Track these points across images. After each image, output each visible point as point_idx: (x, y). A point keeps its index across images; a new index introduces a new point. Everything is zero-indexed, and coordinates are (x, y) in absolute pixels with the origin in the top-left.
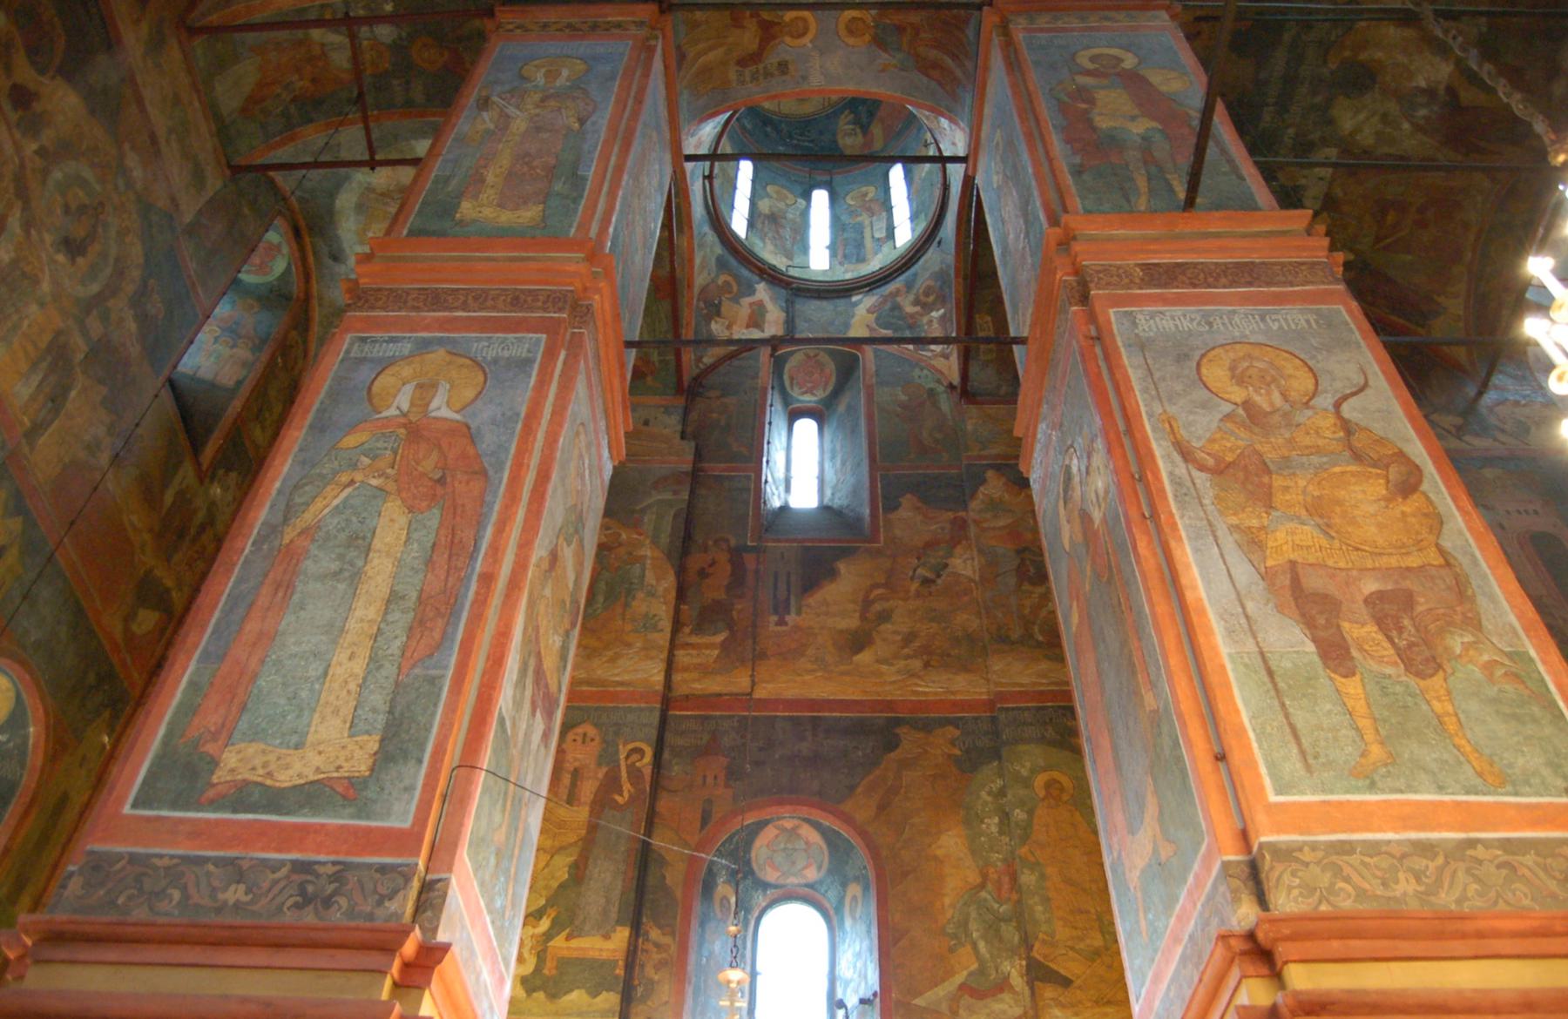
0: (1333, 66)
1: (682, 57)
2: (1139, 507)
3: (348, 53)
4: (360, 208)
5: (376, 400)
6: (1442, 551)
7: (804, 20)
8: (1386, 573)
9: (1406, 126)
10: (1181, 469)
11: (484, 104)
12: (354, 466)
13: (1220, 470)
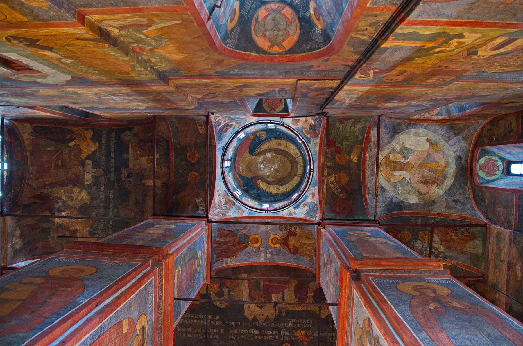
0: (94, 213)
3: (433, 239)
4: (445, 177)
7: (272, 243)
9: (64, 198)
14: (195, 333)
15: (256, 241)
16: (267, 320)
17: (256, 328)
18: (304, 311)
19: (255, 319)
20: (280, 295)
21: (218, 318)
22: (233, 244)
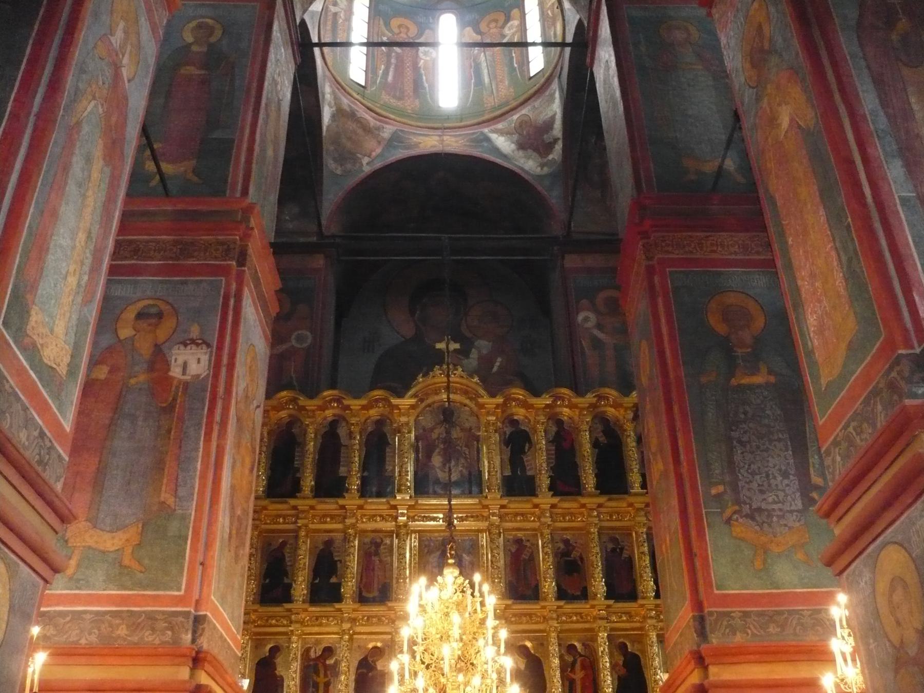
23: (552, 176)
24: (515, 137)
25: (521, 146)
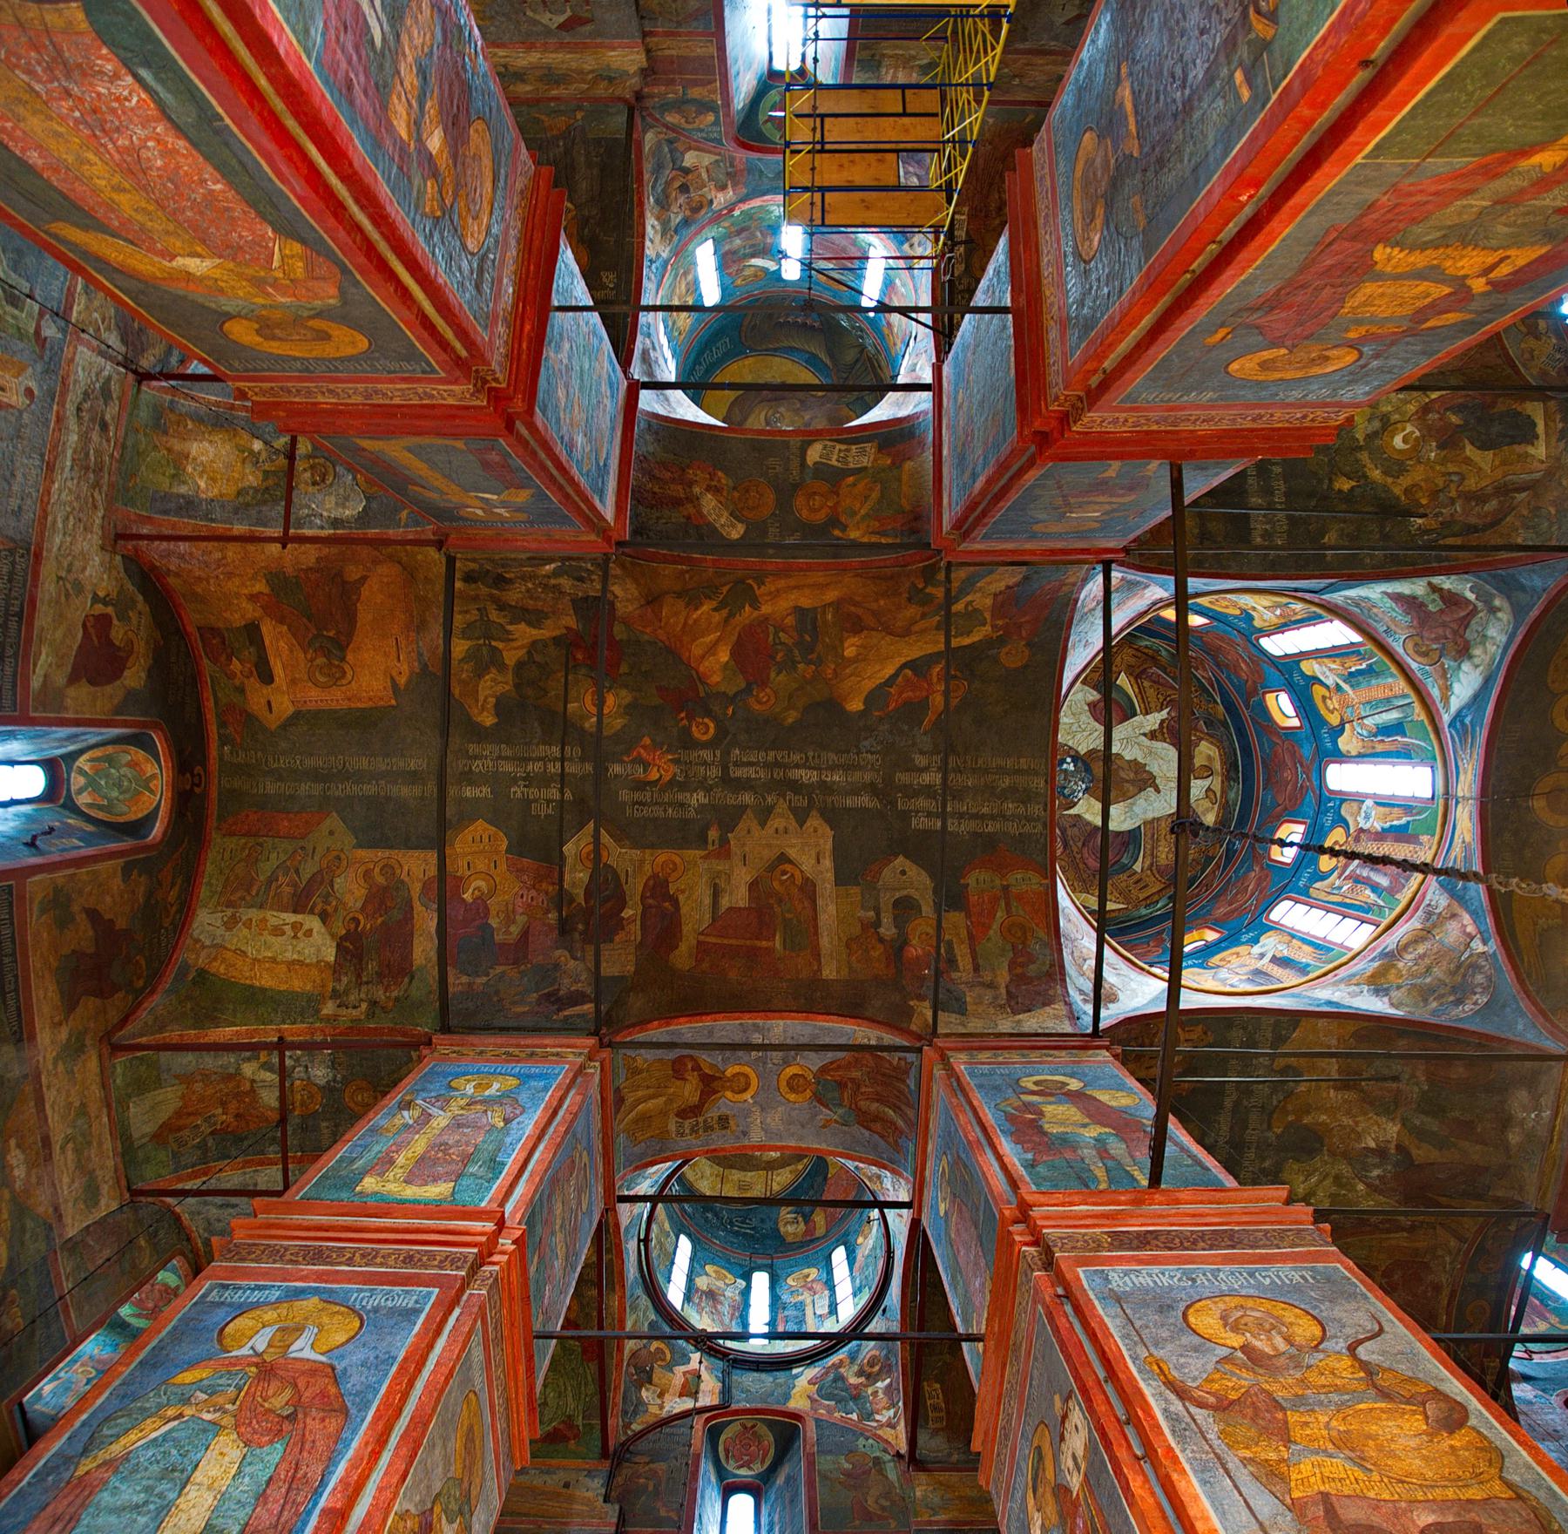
1: (620, 1101)
2: (1129, 1446)
5: (227, 1341)
6: (1509, 1485)
7: (746, 1076)
8: (1443, 1505)
10: (1177, 1406)
11: (408, 1105)
12: (186, 1401)
13: (1222, 1407)
14: (986, 771)
15: (794, 1084)
16: (764, 815)
17: (796, 787)
18: (653, 846)
19: (801, 817)
20: (725, 902)
21: (914, 822)
22: (859, 1087)
23: (1509, 588)
24: (1448, 663)
25: (1464, 652)
